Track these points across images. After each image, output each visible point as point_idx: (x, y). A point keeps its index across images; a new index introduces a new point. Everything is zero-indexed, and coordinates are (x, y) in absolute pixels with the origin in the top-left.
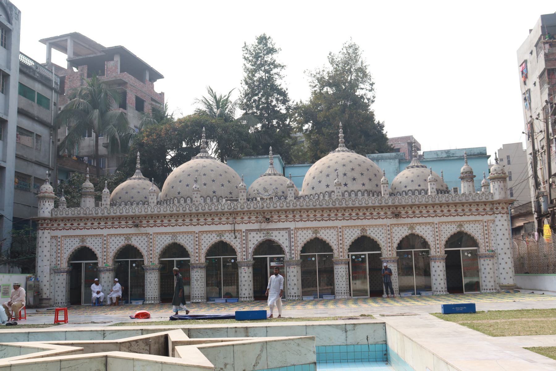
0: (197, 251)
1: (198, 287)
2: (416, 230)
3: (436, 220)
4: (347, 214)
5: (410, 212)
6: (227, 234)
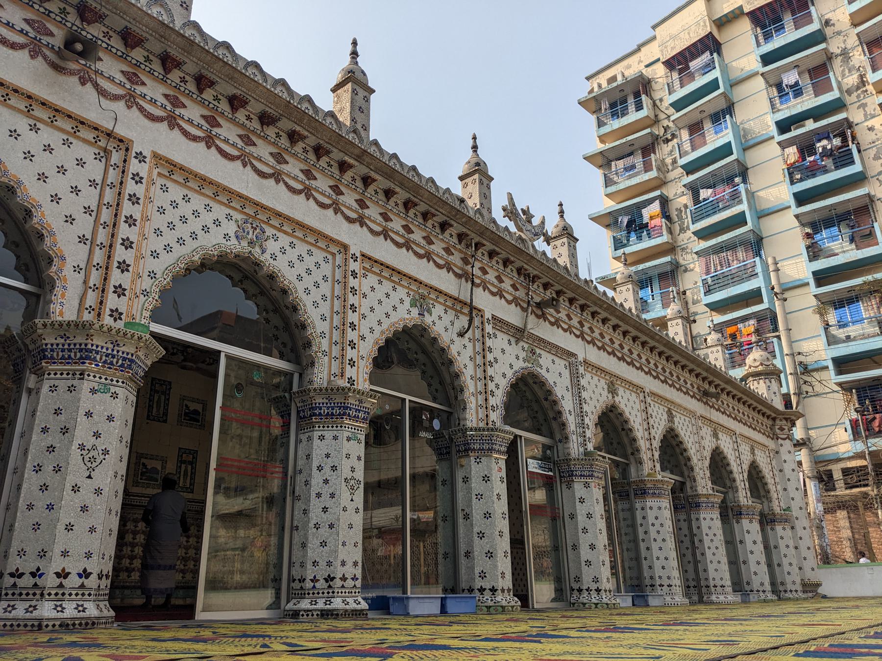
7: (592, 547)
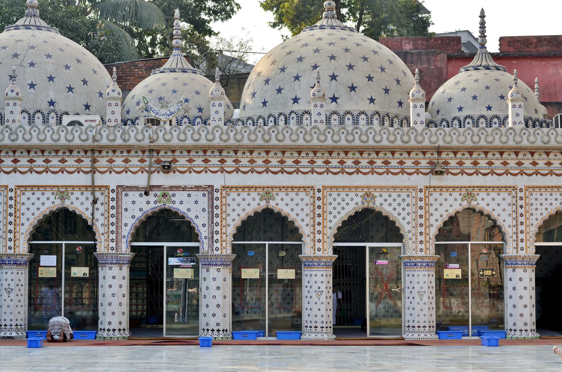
0: (11, 227)
1: (11, 304)
2: (479, 200)
3: (522, 182)
4: (334, 162)
5: (468, 163)
6: (77, 194)
7: (207, 306)
